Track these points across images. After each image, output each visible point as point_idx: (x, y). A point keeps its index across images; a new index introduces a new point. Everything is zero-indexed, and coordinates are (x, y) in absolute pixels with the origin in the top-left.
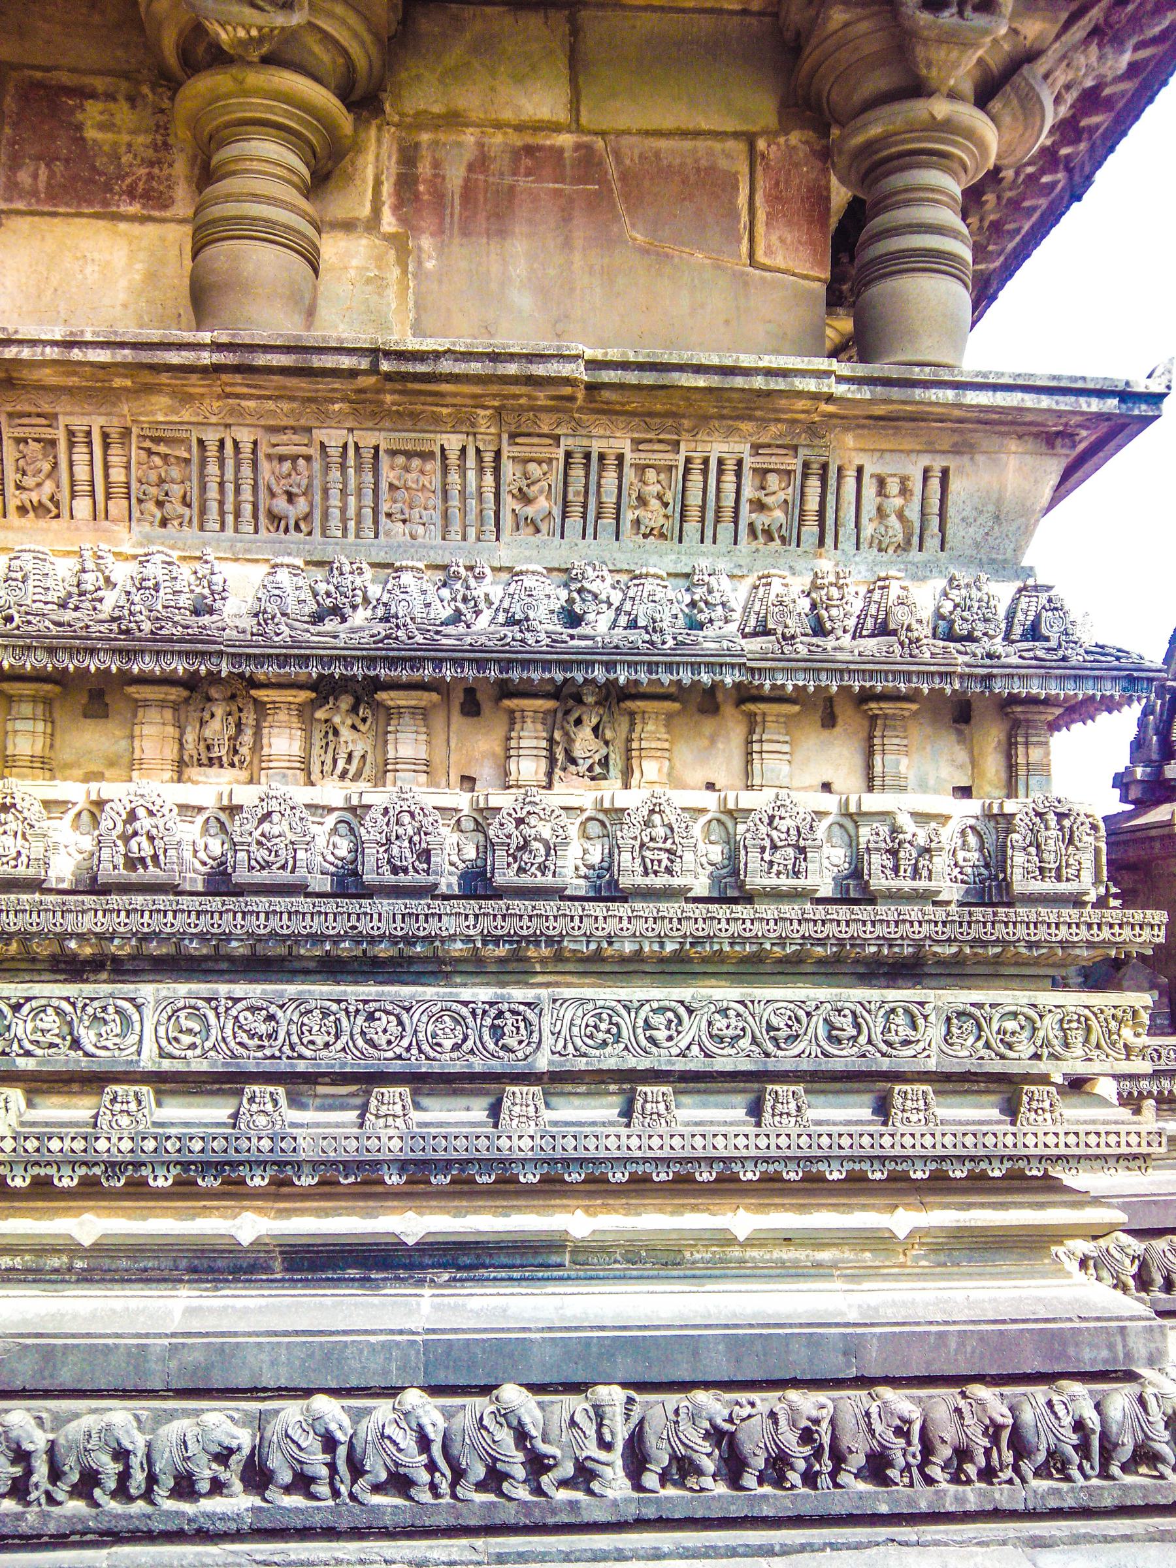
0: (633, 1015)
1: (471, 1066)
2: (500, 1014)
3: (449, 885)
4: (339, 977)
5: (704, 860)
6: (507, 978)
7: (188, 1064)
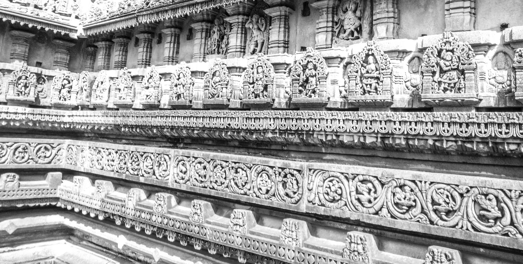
0: (351, 182)
1: (272, 203)
2: (285, 176)
3: (280, 103)
4: (250, 151)
5: (408, 84)
6: (313, 155)
7: (180, 186)
